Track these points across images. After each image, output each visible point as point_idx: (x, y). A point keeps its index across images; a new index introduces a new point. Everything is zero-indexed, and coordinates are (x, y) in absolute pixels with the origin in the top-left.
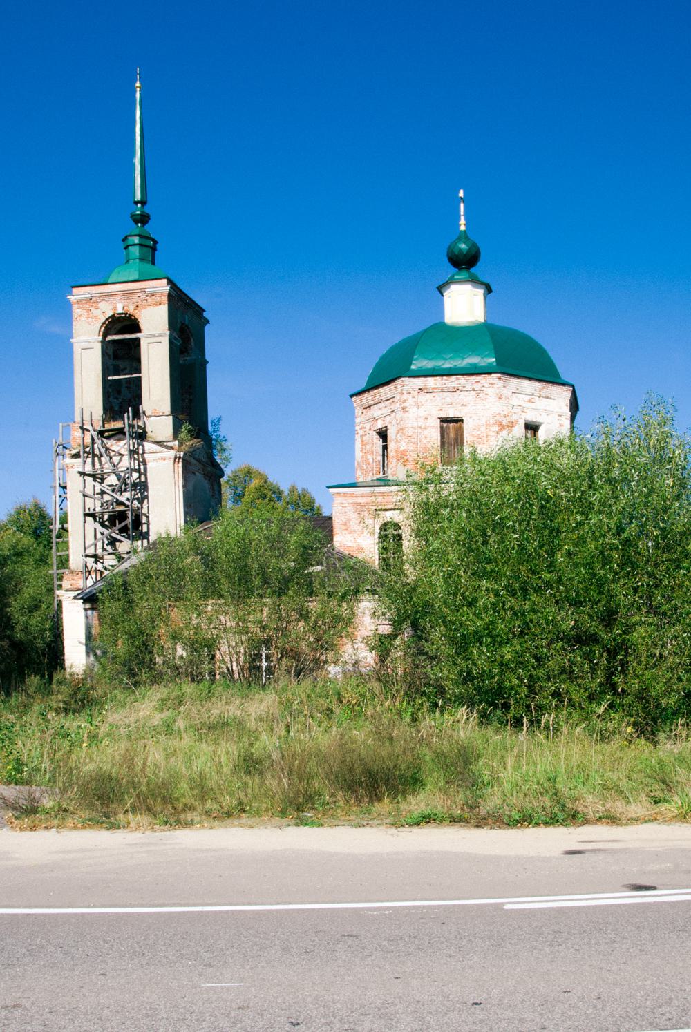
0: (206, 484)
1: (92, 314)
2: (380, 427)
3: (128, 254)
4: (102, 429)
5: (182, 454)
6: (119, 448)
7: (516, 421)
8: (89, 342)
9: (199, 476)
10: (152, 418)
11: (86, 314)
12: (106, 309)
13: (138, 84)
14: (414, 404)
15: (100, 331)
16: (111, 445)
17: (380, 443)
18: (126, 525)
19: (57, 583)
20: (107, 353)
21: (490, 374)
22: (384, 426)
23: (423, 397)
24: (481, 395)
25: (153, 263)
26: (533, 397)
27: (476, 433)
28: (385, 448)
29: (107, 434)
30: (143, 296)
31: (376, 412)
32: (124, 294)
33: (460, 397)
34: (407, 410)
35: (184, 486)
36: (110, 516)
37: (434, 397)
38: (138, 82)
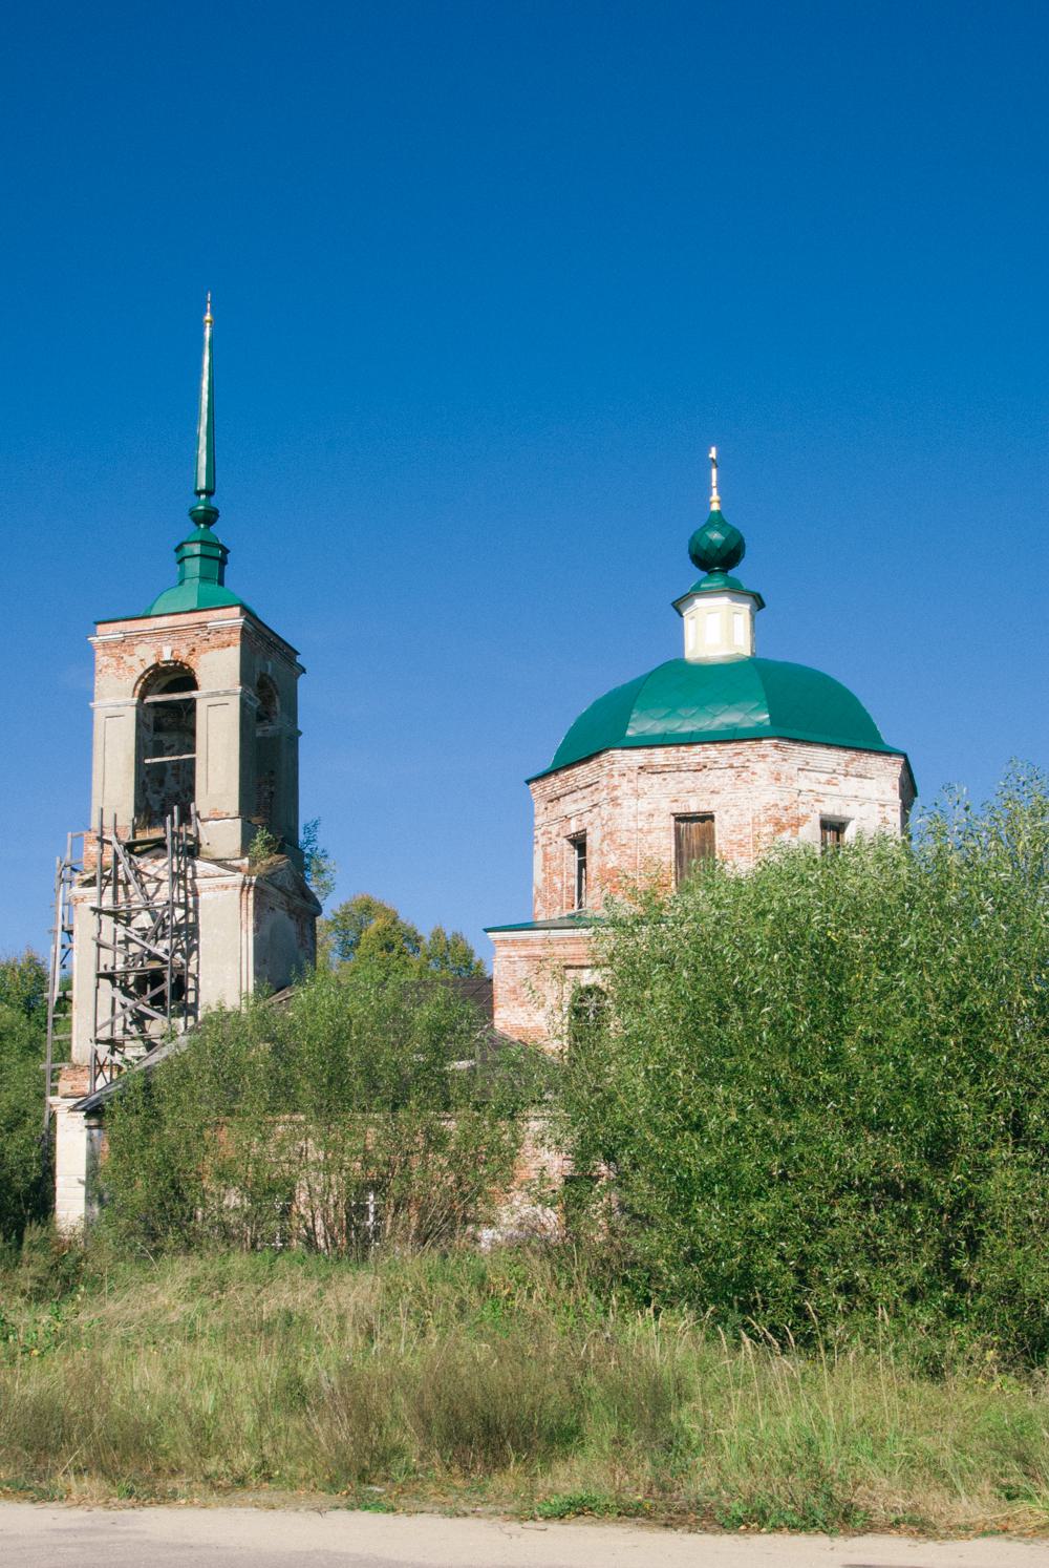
0: (292, 926)
2: (574, 830)
3: (183, 572)
4: (131, 840)
5: (254, 878)
6: (157, 869)
7: (806, 817)
8: (118, 706)
9: (281, 913)
10: (210, 822)
11: (115, 664)
12: (146, 655)
14: (630, 792)
15: (134, 690)
16: (145, 866)
17: (575, 856)
18: (163, 991)
19: (49, 1084)
20: (145, 724)
21: (758, 739)
22: (581, 829)
23: (645, 782)
24: (744, 775)
25: (221, 582)
26: (834, 775)
27: (735, 837)
28: (582, 865)
29: (138, 848)
30: (203, 634)
31: (568, 806)
32: (174, 631)
34: (619, 801)
35: (256, 930)
36: (138, 979)
37: (665, 779)
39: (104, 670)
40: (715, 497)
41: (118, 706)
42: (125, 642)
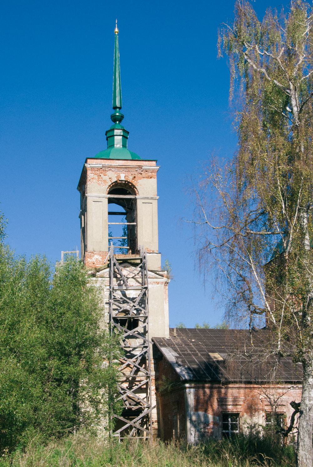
1: (102, 178)
8: (100, 197)
11: (97, 178)
12: (112, 177)
13: (117, 30)
32: (126, 168)
38: (116, 29)
39: (91, 180)
41: (100, 197)
42: (103, 169)
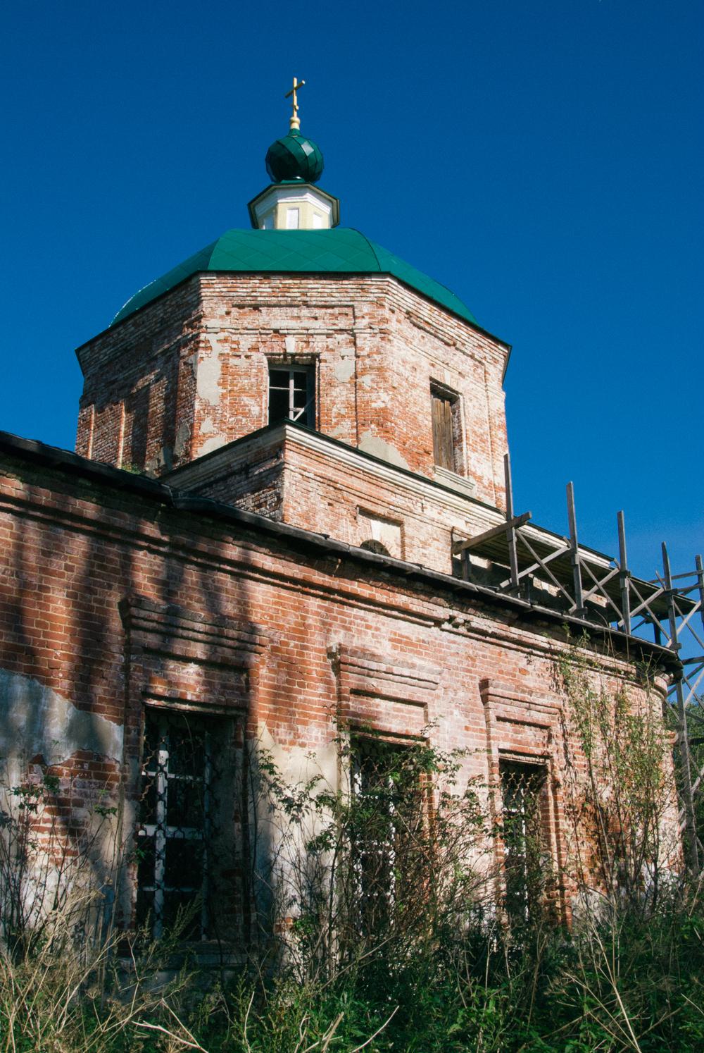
33: (456, 358)
40: (296, 118)
